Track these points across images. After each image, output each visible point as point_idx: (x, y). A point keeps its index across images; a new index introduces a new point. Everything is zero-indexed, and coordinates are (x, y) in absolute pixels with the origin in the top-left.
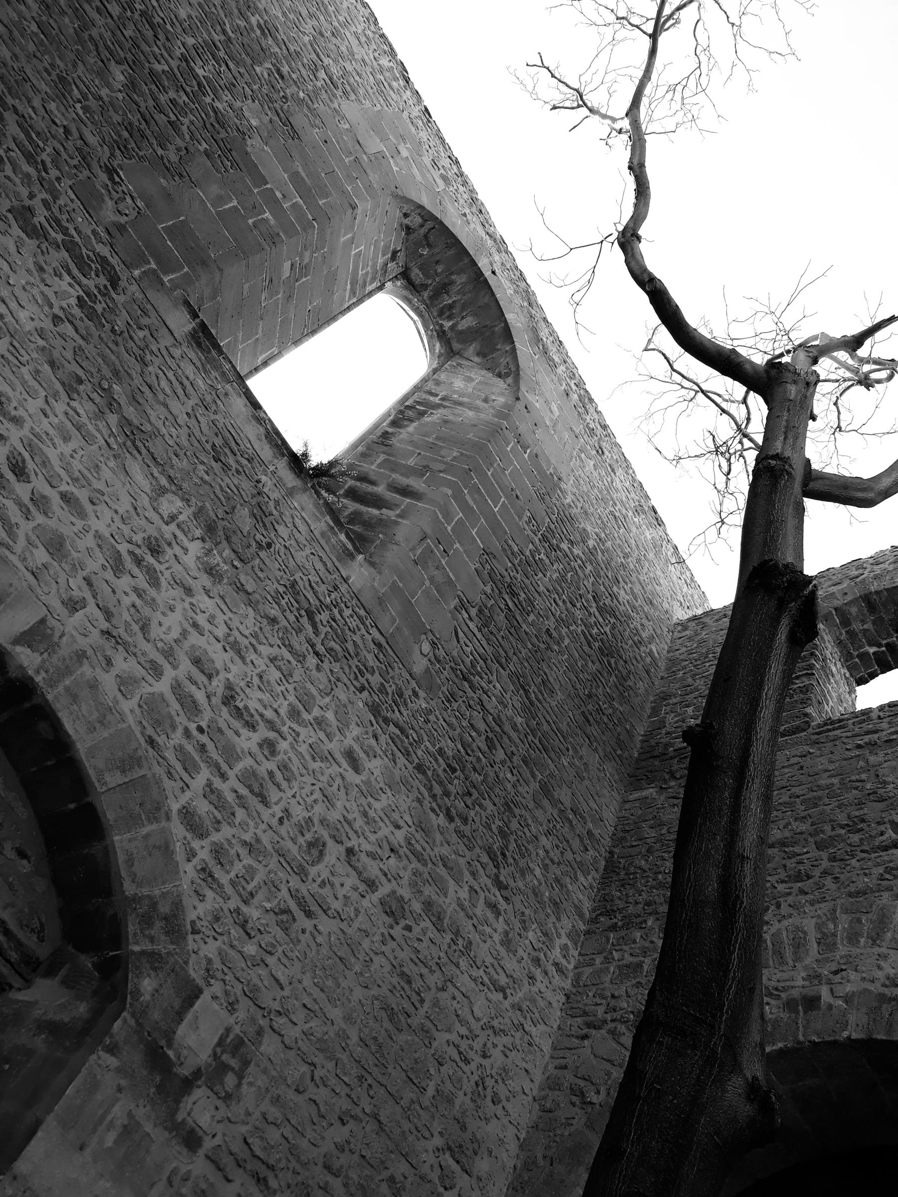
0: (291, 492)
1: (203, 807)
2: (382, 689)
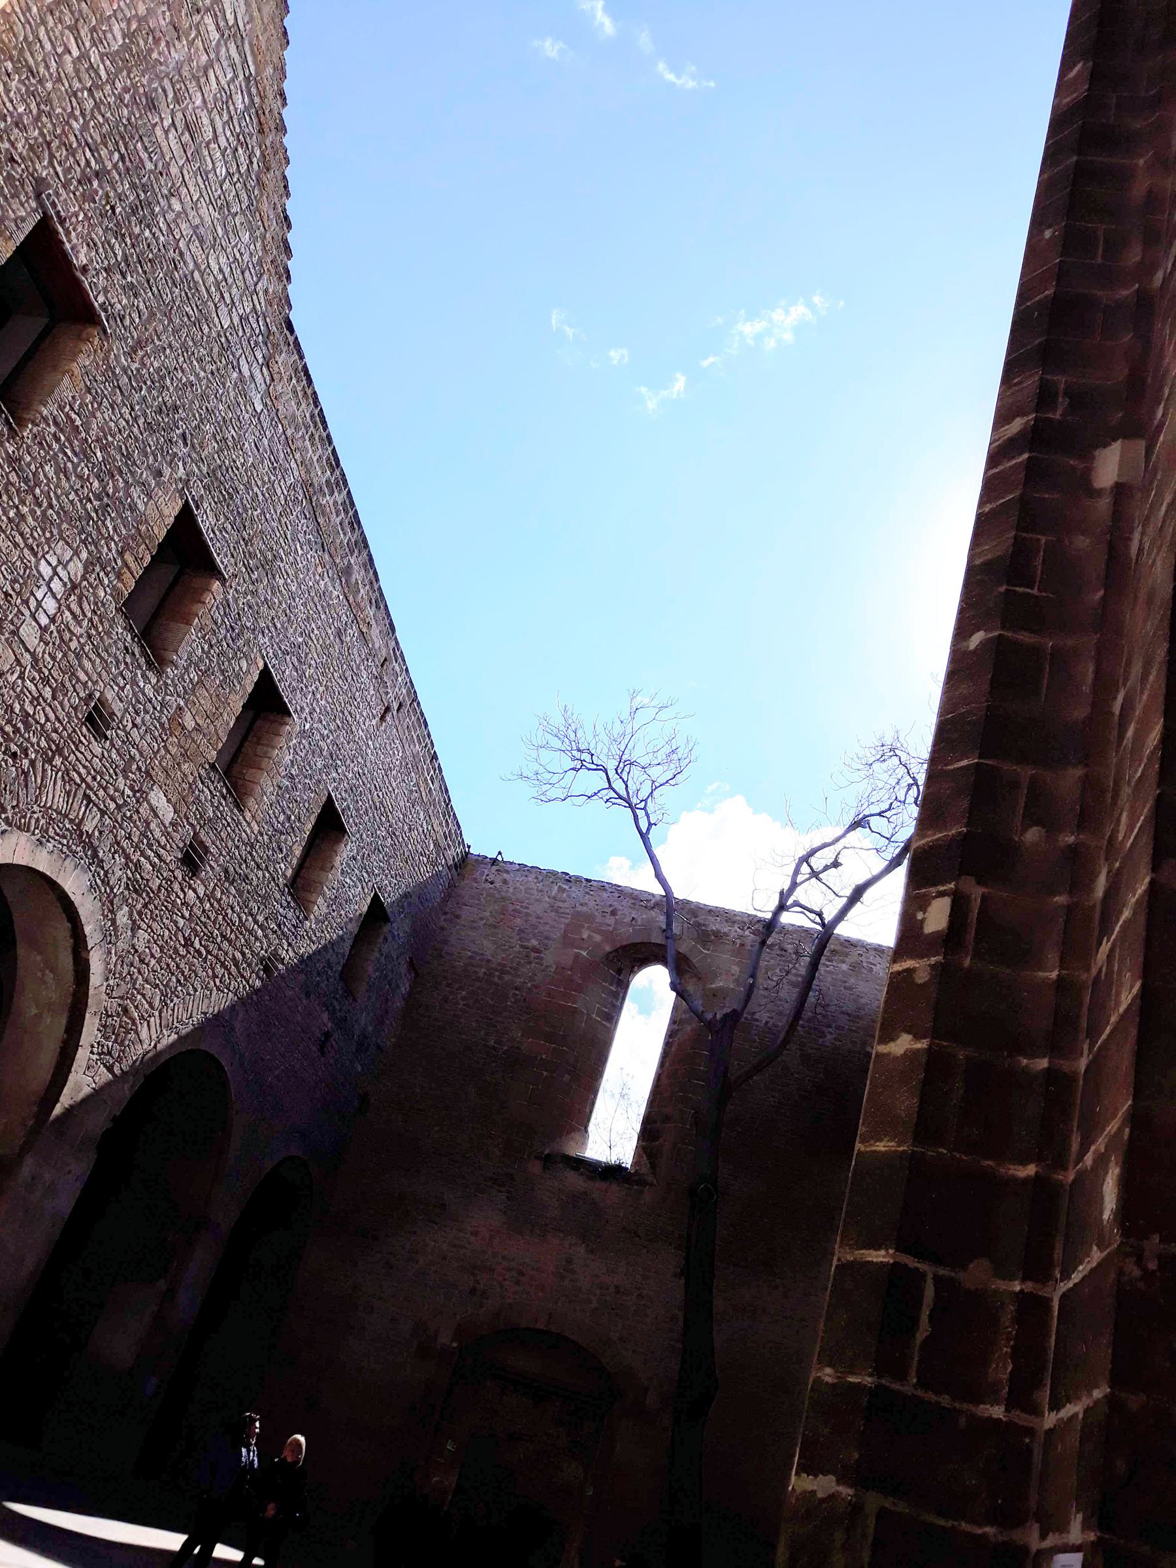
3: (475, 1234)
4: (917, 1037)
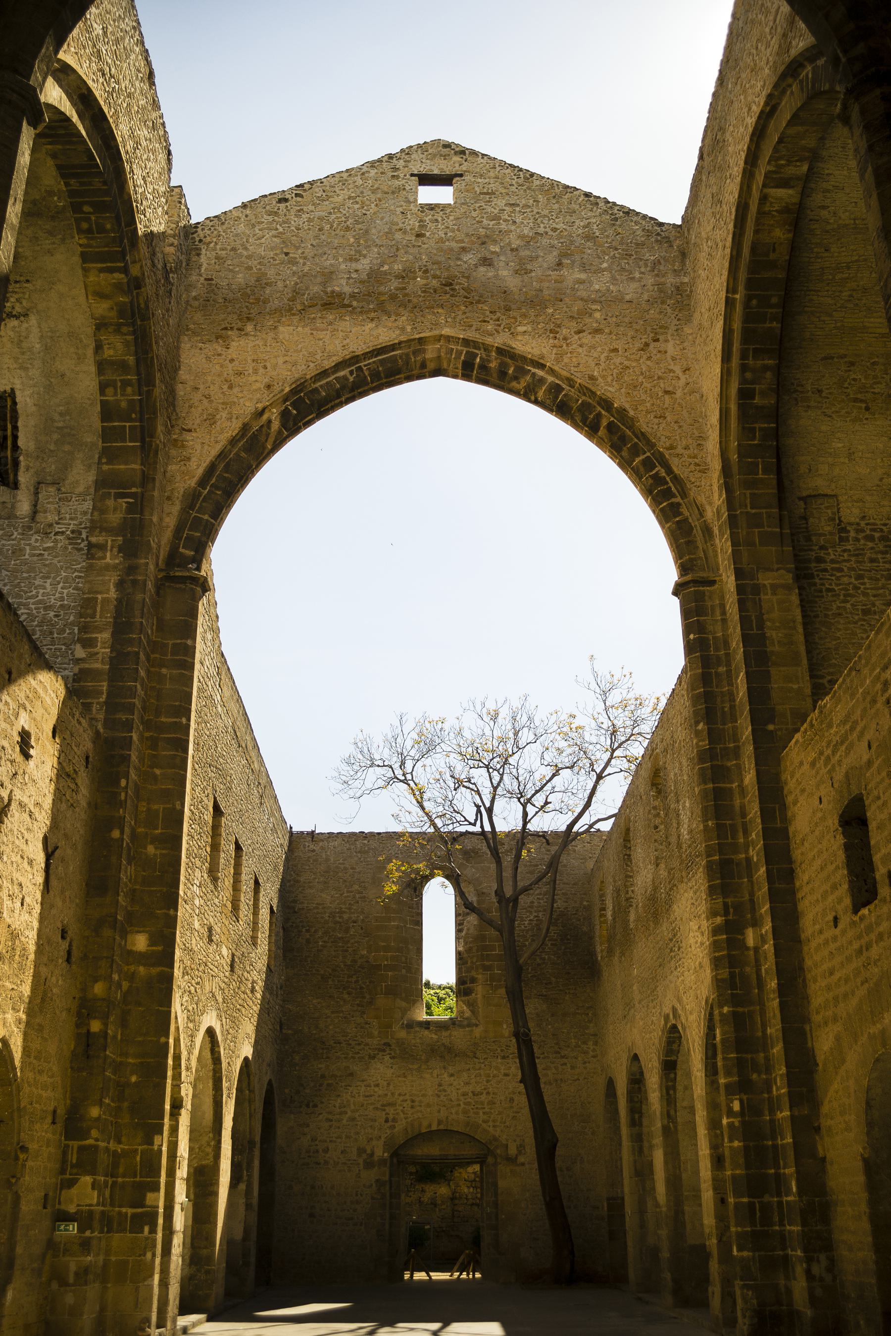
0: (450, 1035)
1: (485, 1117)
2: (502, 1050)
3: (377, 1085)
4: (740, 1142)
